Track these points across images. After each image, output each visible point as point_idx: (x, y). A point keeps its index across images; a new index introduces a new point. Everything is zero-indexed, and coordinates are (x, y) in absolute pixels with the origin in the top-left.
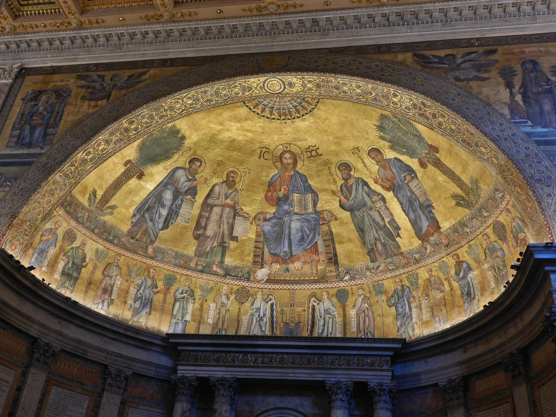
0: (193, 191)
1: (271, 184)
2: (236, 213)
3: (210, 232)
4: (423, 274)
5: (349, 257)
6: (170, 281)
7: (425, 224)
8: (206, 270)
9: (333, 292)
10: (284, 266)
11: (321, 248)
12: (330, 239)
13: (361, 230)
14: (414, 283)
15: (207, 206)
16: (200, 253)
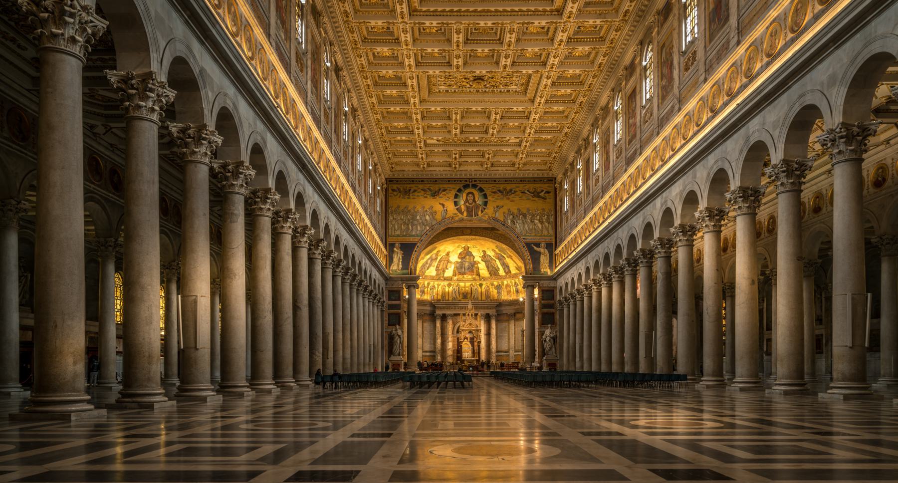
0: (436, 259)
1: (460, 254)
2: (448, 261)
3: (440, 268)
4: (505, 282)
5: (483, 274)
6: (429, 284)
7: (507, 270)
8: (439, 279)
9: (478, 283)
10: (462, 276)
11: (475, 271)
12: (478, 269)
13: (488, 267)
14: (503, 284)
15: (440, 261)
16: (437, 275)
